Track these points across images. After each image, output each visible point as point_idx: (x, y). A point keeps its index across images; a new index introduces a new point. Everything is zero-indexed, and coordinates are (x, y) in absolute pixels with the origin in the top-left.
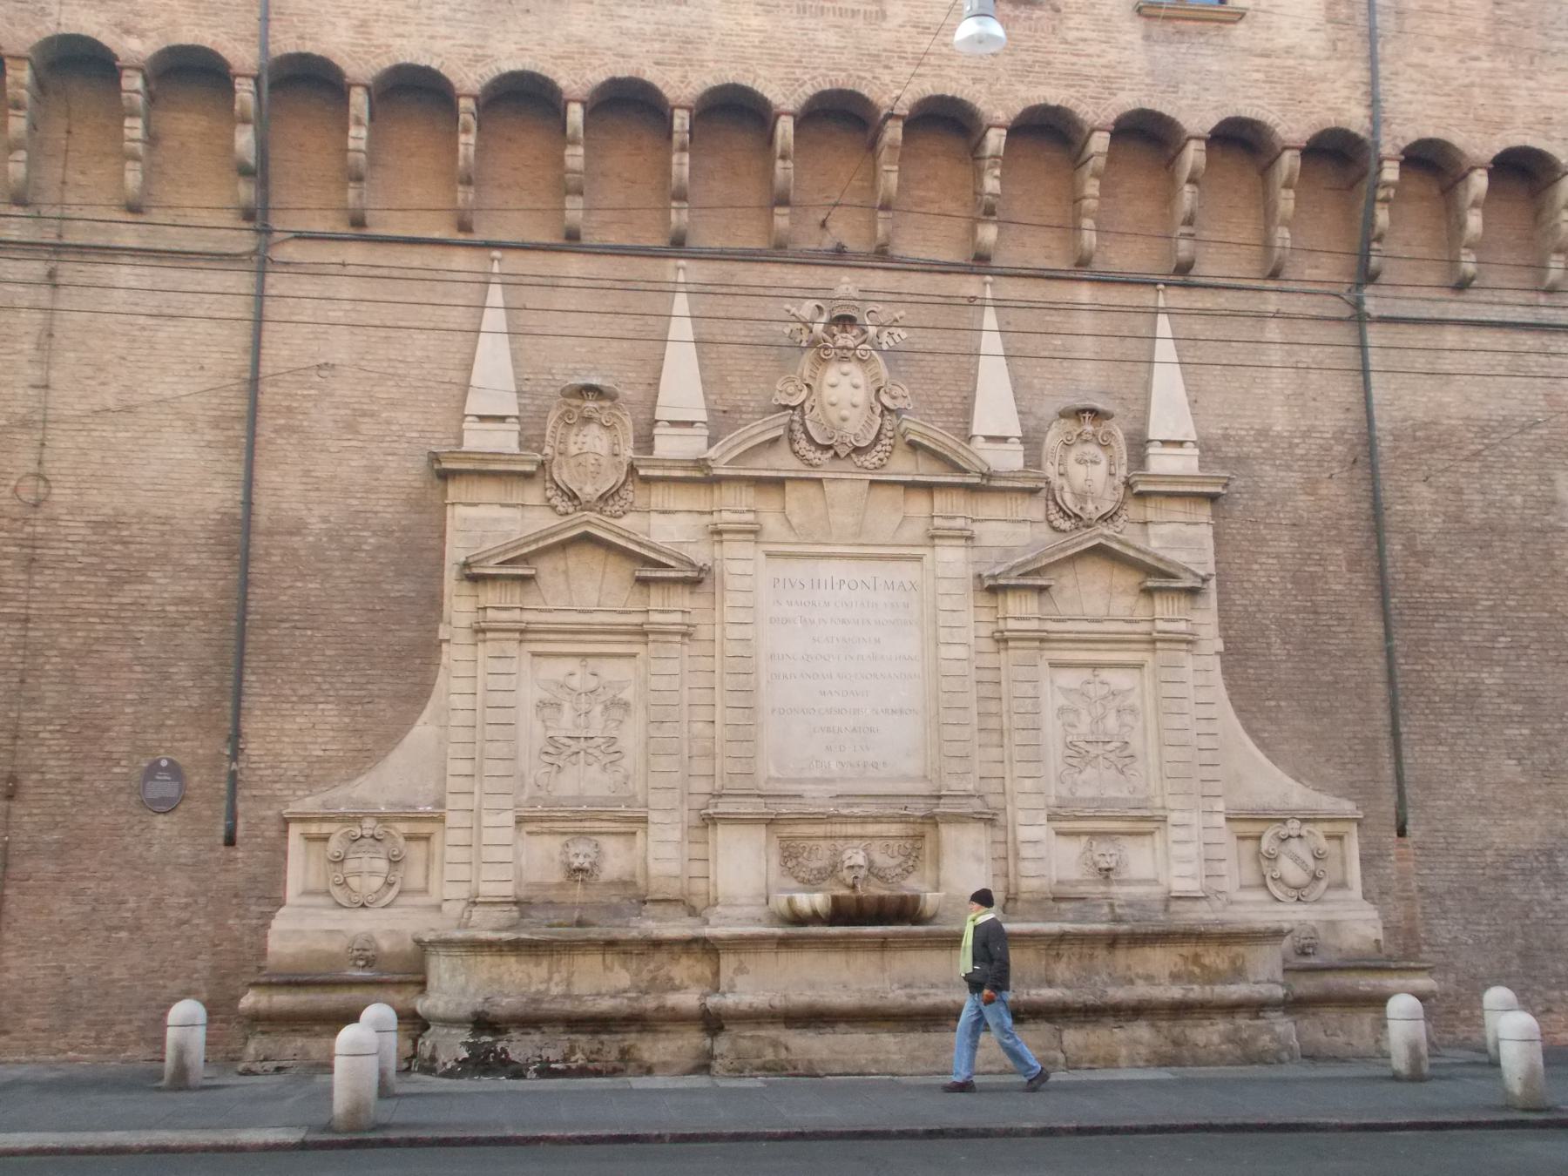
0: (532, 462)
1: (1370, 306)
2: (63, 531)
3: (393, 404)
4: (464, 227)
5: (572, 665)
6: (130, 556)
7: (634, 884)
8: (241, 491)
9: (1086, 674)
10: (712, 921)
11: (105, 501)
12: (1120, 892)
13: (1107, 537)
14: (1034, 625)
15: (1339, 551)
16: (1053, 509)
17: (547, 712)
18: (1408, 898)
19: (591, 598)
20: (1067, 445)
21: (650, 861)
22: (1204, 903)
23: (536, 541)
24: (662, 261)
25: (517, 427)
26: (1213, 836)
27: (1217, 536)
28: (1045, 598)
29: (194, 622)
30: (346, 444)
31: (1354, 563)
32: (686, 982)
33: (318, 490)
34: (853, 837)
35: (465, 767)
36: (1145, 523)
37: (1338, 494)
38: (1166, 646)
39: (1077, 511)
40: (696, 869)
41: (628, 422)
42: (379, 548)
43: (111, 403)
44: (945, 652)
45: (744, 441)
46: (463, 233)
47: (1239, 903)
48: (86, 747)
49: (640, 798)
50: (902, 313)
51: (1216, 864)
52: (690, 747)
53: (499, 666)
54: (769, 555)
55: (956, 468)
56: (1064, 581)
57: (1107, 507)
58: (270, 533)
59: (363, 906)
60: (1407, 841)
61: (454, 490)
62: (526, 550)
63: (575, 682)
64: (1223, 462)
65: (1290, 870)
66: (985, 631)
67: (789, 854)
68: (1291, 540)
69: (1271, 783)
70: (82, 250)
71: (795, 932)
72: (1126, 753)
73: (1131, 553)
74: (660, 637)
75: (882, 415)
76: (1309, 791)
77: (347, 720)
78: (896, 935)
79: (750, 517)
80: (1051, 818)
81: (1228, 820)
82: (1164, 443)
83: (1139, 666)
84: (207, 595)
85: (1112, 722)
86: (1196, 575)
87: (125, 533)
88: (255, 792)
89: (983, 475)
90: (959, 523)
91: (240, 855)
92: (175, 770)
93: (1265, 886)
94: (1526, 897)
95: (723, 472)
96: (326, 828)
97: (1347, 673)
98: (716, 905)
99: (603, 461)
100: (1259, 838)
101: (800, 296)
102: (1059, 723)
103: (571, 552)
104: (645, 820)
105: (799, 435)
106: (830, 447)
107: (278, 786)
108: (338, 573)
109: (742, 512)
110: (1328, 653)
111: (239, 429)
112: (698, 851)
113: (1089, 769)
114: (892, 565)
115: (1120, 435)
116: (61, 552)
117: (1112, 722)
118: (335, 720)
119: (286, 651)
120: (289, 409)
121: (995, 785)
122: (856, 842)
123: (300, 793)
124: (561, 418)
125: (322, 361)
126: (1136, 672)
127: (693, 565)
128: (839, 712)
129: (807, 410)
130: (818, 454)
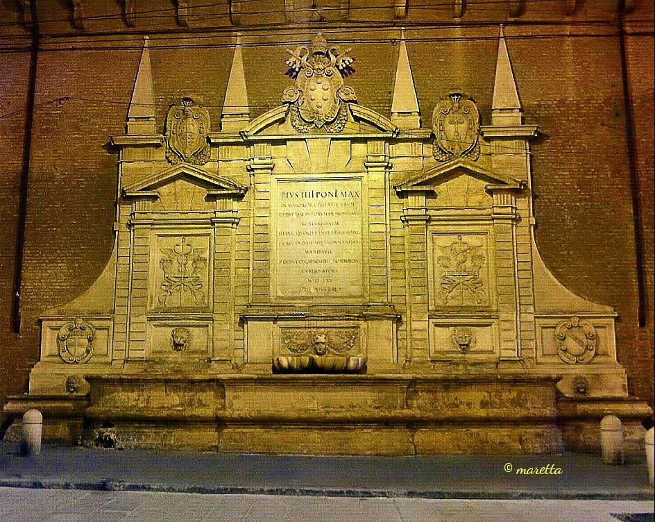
1: (628, 29)
10: (243, 371)
12: (470, 357)
14: (423, 212)
18: (645, 361)
19: (188, 206)
31: (616, 172)
33: (60, 159)
35: (125, 293)
39: (450, 150)
40: (239, 344)
44: (373, 228)
46: (130, 27)
47: (542, 364)
54: (279, 180)
58: (37, 181)
59: (76, 362)
63: (179, 249)
64: (537, 120)
71: (281, 376)
78: (320, 379)
81: (535, 317)
84: (9, 212)
85: (469, 264)
89: (394, 132)
96: (59, 323)
97: (611, 234)
99: (195, 137)
100: (555, 327)
106: (313, 122)
112: (239, 335)
122: (322, 330)
123: (49, 307)
127: (236, 186)
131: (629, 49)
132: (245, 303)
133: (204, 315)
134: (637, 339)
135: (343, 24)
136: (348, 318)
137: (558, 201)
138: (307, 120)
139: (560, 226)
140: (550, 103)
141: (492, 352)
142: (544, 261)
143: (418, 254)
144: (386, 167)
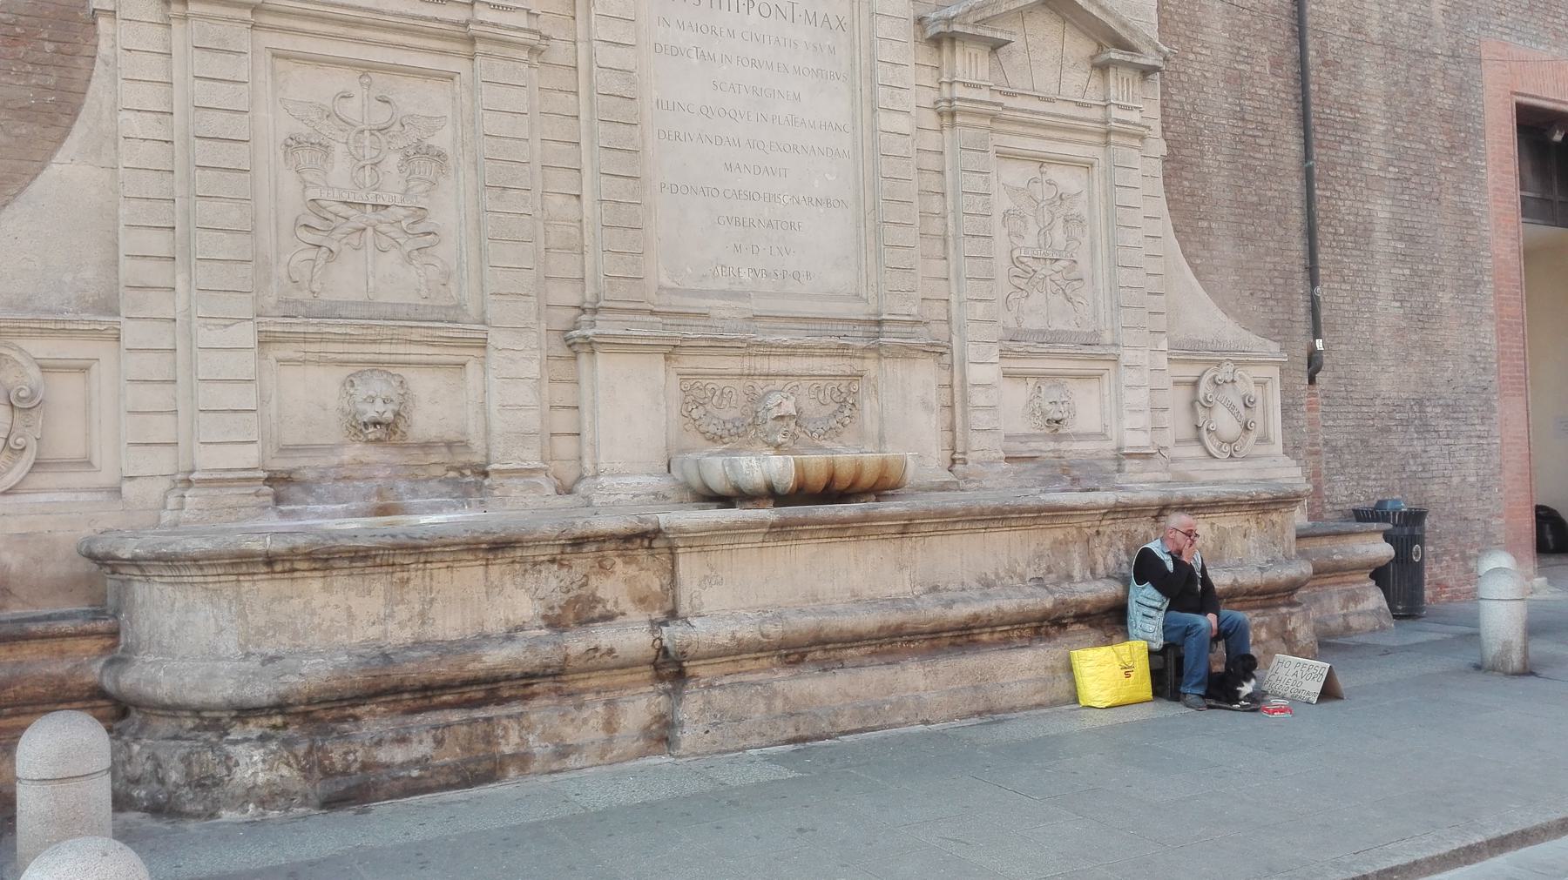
5: (345, 80)
7: (465, 445)
9: (1033, 168)
12: (1075, 449)
14: (985, 95)
17: (304, 156)
18: (1316, 453)
21: (494, 408)
31: (1276, 64)
32: (626, 605)
35: (158, 243)
38: (1121, 140)
40: (562, 421)
44: (885, 121)
49: (472, 309)
60: (1317, 389)
63: (351, 109)
66: (928, 98)
67: (693, 399)
69: (1207, 319)
72: (1073, 275)
74: (496, 50)
83: (1088, 166)
85: (1059, 235)
86: (1159, 51)
93: (1199, 440)
94: (1404, 449)
97: (1269, 194)
100: (1195, 384)
104: (483, 345)
112: (563, 394)
117: (1059, 235)
121: (938, 310)
128: (751, 197)
132: (576, 301)
133: (458, 337)
134: (1304, 408)
136: (842, 351)
141: (1102, 436)
143: (978, 198)
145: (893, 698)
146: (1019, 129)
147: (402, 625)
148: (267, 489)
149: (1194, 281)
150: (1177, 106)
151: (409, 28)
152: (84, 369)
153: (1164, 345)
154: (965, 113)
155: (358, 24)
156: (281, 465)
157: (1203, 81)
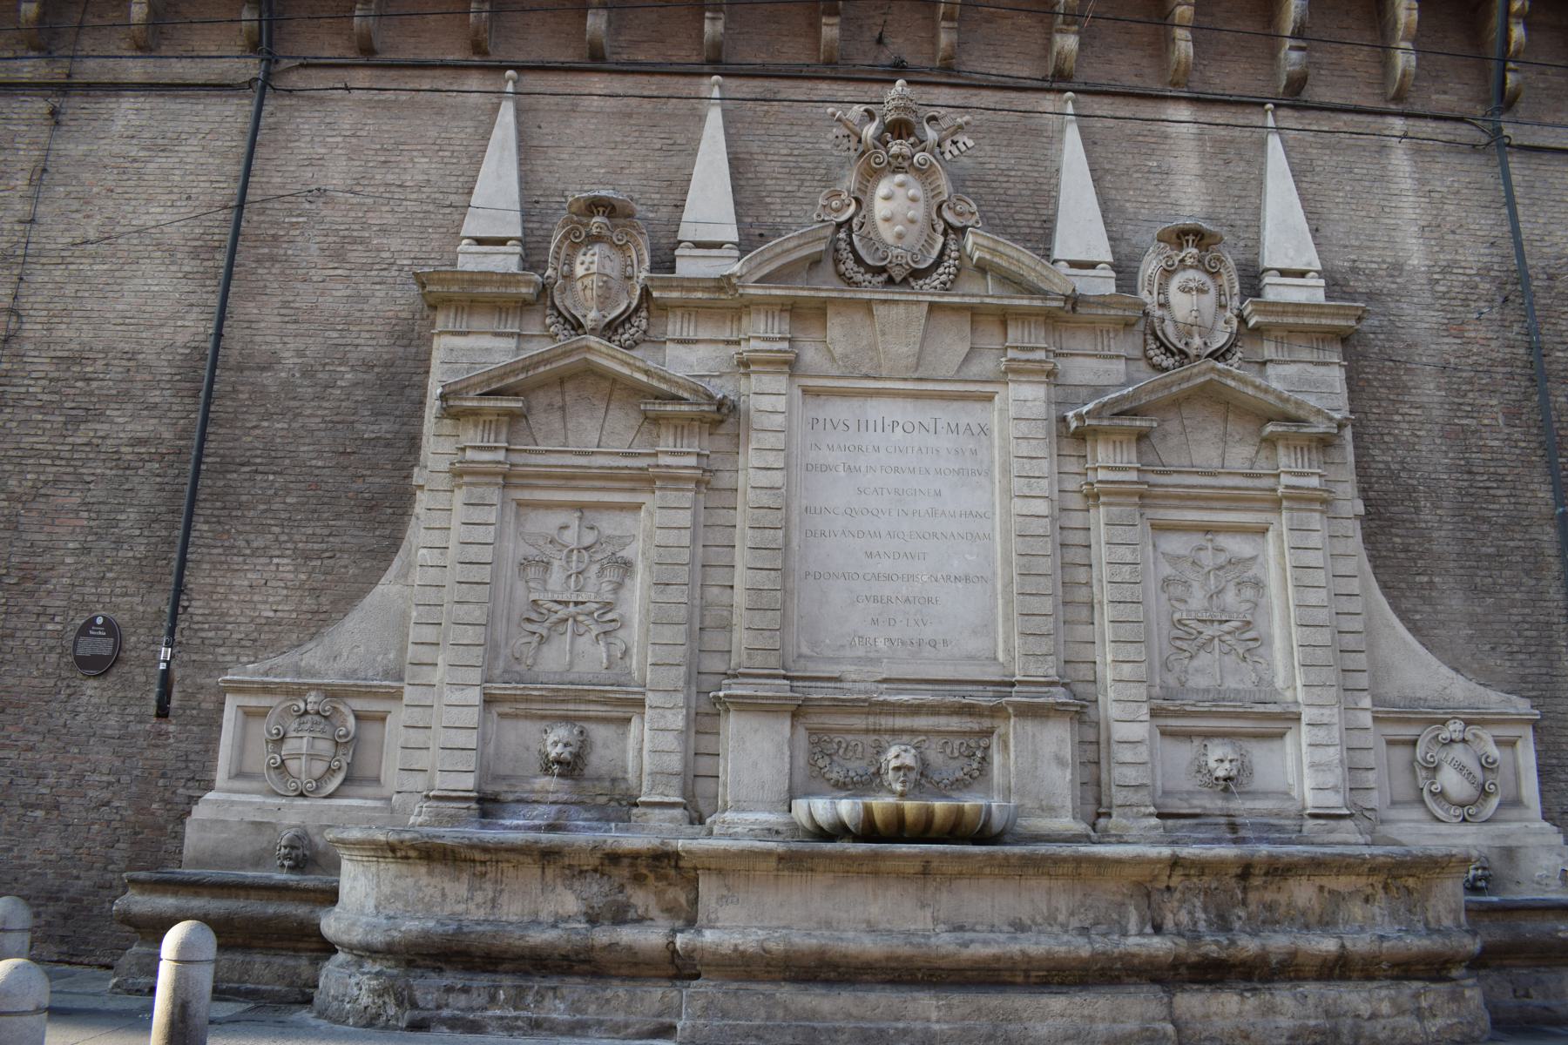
0: (528, 283)
2: (28, 368)
3: (384, 230)
4: (478, 47)
6: (91, 394)
8: (213, 324)
9: (1197, 539)
11: (71, 335)
13: (1219, 371)
14: (1133, 476)
15: (1494, 402)
16: (1152, 345)
17: (532, 572)
19: (591, 439)
20: (1168, 273)
22: (1349, 824)
23: (526, 369)
24: (695, 80)
25: (518, 249)
26: (1358, 740)
27: (1349, 379)
28: (1144, 447)
29: (148, 465)
30: (332, 272)
31: (1512, 415)
33: (296, 322)
34: (902, 731)
35: (429, 633)
36: (1264, 363)
37: (1489, 338)
39: (1181, 346)
41: (644, 244)
42: (356, 385)
43: (92, 235)
45: (777, 256)
48: (23, 600)
50: (967, 118)
51: (1365, 774)
52: (702, 616)
53: (478, 515)
54: (806, 391)
55: (1033, 291)
56: (1167, 426)
57: (1220, 340)
59: (302, 795)
61: (442, 320)
62: (512, 380)
63: (570, 537)
65: (1452, 781)
68: (1439, 388)
69: (1422, 673)
70: (89, 87)
72: (1247, 635)
73: (1250, 391)
75: (945, 233)
76: (1473, 685)
77: (303, 577)
79: (785, 345)
80: (1155, 713)
81: (1375, 719)
82: (1283, 273)
84: (166, 435)
85: (1230, 597)
86: (1331, 419)
87: (89, 369)
88: (194, 657)
90: (1041, 355)
91: (171, 728)
92: (111, 628)
93: (1423, 802)
95: (752, 291)
97: (1512, 544)
98: (724, 811)
100: (1414, 743)
101: (851, 111)
102: (1166, 596)
103: (569, 386)
105: (845, 254)
106: (883, 270)
107: (221, 650)
108: (309, 412)
109: (773, 340)
110: (1486, 520)
111: (221, 259)
113: (1202, 653)
114: (956, 405)
115: (1231, 263)
116: (23, 390)
118: (291, 576)
119: (244, 498)
120: (275, 237)
122: (906, 738)
123: (244, 659)
124: (566, 237)
125: (313, 187)
126: (1258, 538)
127: (710, 397)
128: (889, 578)
129: (855, 228)
130: (868, 277)
131: (1516, 178)
132: (722, 668)
135: (944, 80)
137: (1404, 469)
138: (870, 262)
139: (1412, 522)
140: (1374, 266)
142: (1385, 595)
143: (1127, 567)
144: (1050, 374)
145: (901, 1025)
146: (1176, 502)
147: (478, 906)
148: (474, 805)
149: (1409, 637)
150: (1381, 466)
151: (609, 477)
152: (383, 719)
153: (1366, 702)
154: (1108, 493)
155: (573, 477)
156: (490, 789)
157: (1412, 439)
